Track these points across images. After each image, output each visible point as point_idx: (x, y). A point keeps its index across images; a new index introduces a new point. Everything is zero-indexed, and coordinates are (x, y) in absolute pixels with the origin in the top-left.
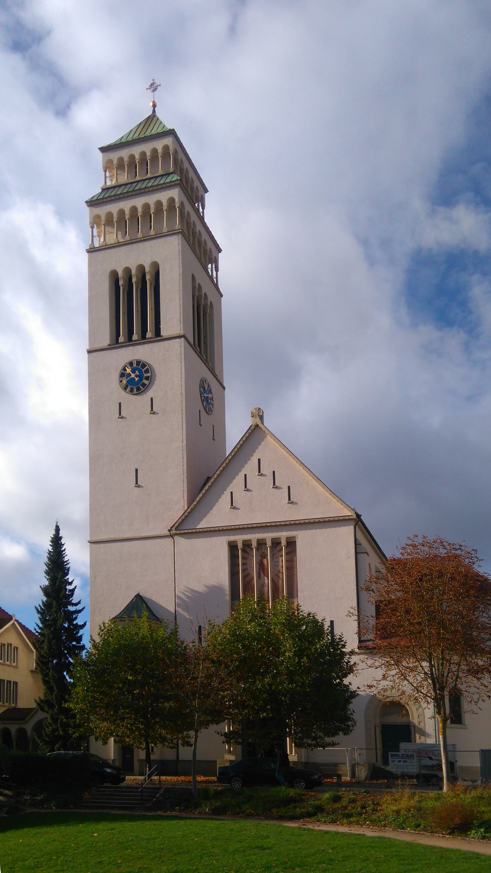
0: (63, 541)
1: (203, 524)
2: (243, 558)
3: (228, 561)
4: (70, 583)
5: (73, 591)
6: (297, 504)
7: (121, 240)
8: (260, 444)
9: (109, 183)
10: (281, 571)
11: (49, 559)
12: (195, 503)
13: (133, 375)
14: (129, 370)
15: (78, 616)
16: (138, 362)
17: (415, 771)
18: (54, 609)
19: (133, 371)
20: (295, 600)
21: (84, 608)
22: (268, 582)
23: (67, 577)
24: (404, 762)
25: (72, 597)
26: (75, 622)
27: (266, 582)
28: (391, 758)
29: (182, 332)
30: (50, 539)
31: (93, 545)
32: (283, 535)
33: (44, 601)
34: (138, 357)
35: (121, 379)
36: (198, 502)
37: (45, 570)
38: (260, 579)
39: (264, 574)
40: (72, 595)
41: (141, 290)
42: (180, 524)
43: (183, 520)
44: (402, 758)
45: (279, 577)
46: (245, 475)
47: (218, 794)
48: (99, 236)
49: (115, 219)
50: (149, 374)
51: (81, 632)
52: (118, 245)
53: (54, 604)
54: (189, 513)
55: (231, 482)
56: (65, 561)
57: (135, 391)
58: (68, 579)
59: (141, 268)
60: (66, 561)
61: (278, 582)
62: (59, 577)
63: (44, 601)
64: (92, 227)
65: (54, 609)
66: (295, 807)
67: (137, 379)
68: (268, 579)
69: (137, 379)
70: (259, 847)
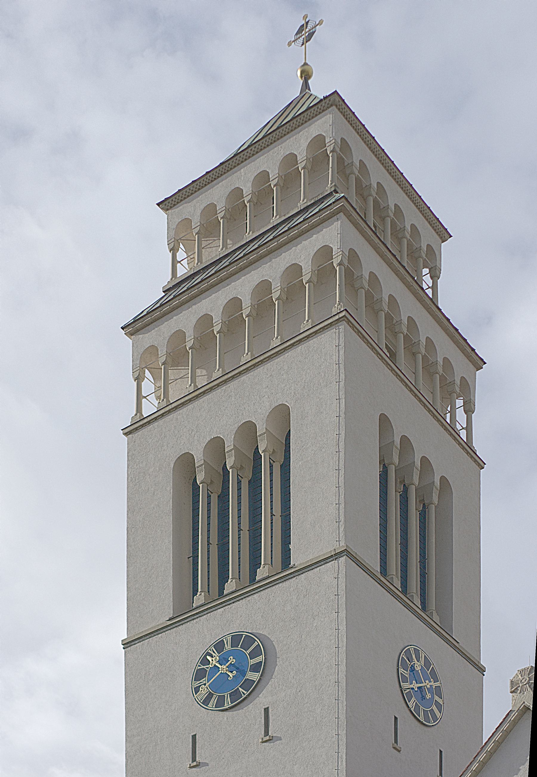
14: (213, 661)
16: (236, 639)
34: (234, 629)
50: (261, 658)
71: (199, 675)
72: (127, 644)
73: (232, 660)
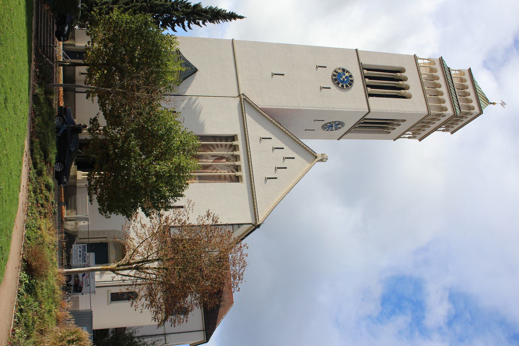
0: (233, 20)
1: (248, 118)
2: (226, 145)
3: (223, 134)
4: (204, 23)
5: (198, 24)
6: (265, 183)
7: (423, 76)
8: (304, 159)
9: (452, 72)
10: (218, 171)
11: (220, 10)
12: (263, 113)
13: (344, 77)
14: (347, 74)
15: (181, 27)
16: (352, 81)
17: (74, 264)
18: (185, 10)
19: (346, 77)
20: (197, 181)
21: (186, 31)
22: (210, 162)
23: (208, 21)
24: (80, 256)
25: (194, 23)
26: (176, 24)
27: (210, 161)
28: (82, 246)
29: (372, 111)
30: (234, 12)
31: (231, 42)
32: (243, 173)
33: (191, 4)
34: (355, 81)
35: (341, 69)
36: (264, 115)
37: (212, 6)
38: (212, 156)
39: (215, 159)
40: (195, 23)
41: (395, 87)
42: (248, 102)
43: (250, 104)
44: (82, 254)
45: (213, 170)
46: (283, 148)
47: (50, 103)
48: (424, 63)
49: (433, 74)
51: (169, 28)
52: (420, 75)
53: (189, 10)
54: (256, 109)
55: (278, 138)
56: (220, 21)
57: (334, 77)
58: (207, 22)
59: (408, 88)
60: (219, 22)
61: (208, 170)
62: (208, 16)
63: (191, 4)
64: (428, 59)
65: (185, 10)
66: (40, 155)
67: (342, 79)
68: (212, 162)
69: (342, 79)
70: (7, 99)
71: (344, 70)
72: (356, 50)
73: (346, 80)
